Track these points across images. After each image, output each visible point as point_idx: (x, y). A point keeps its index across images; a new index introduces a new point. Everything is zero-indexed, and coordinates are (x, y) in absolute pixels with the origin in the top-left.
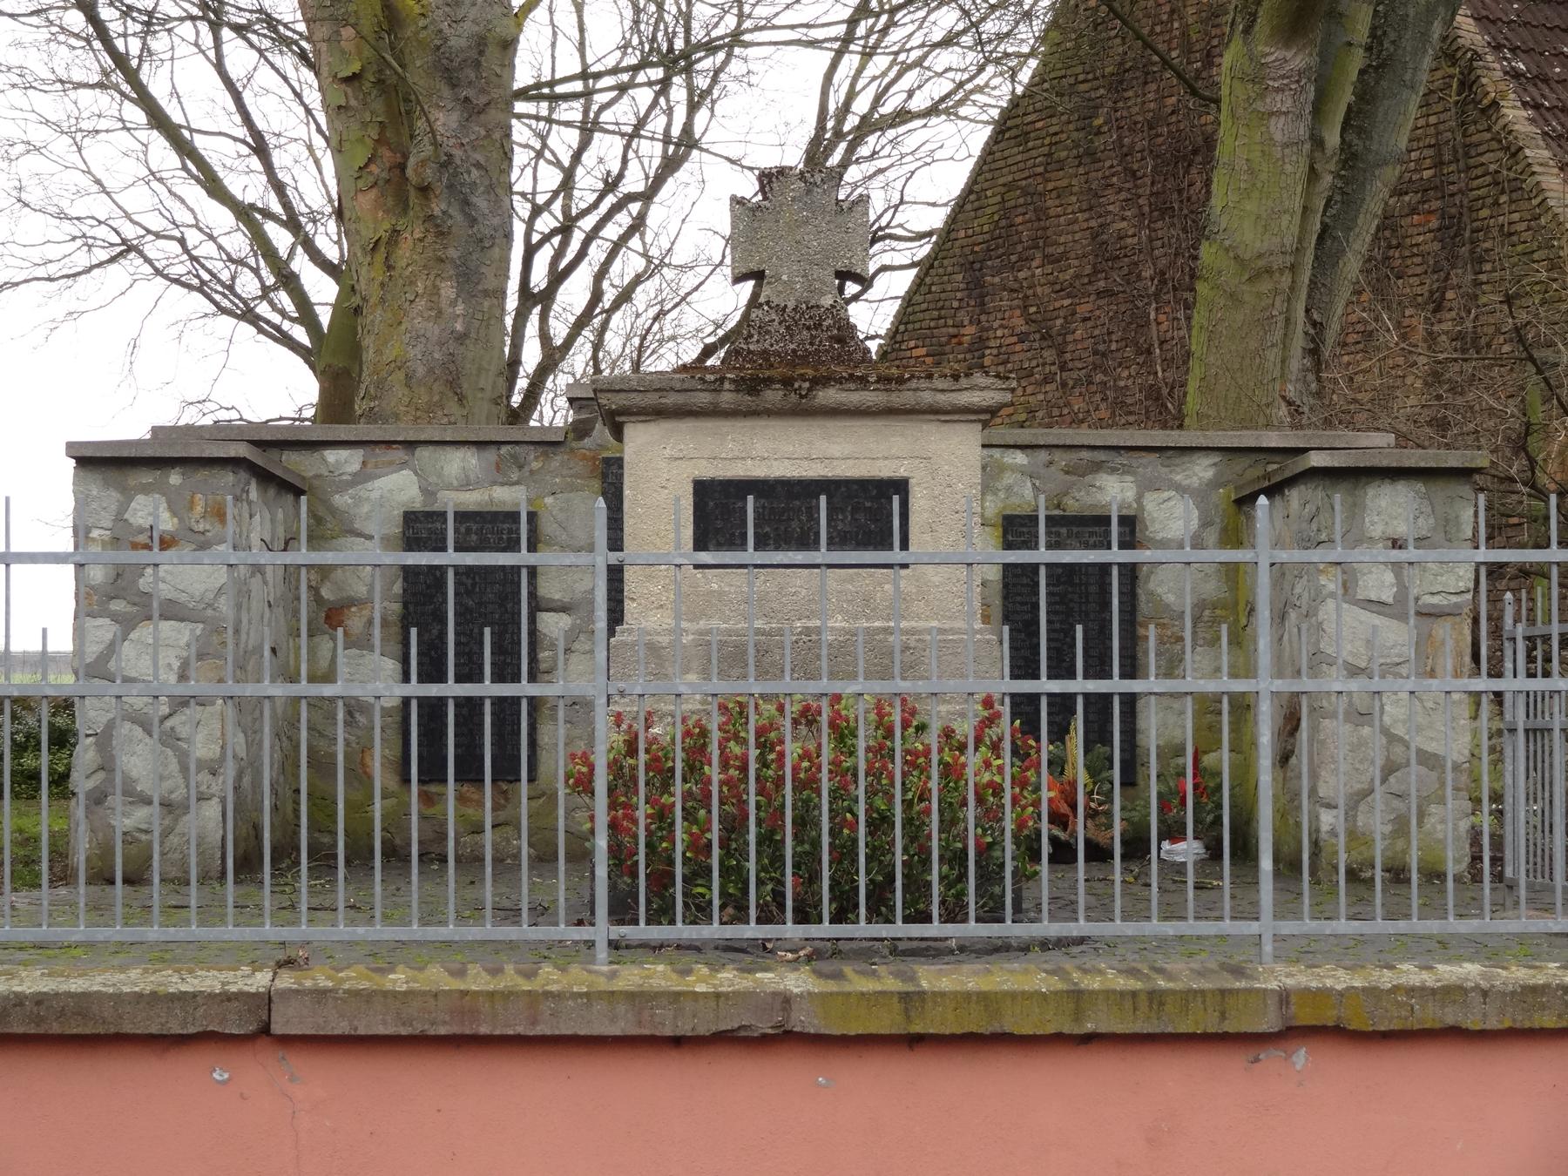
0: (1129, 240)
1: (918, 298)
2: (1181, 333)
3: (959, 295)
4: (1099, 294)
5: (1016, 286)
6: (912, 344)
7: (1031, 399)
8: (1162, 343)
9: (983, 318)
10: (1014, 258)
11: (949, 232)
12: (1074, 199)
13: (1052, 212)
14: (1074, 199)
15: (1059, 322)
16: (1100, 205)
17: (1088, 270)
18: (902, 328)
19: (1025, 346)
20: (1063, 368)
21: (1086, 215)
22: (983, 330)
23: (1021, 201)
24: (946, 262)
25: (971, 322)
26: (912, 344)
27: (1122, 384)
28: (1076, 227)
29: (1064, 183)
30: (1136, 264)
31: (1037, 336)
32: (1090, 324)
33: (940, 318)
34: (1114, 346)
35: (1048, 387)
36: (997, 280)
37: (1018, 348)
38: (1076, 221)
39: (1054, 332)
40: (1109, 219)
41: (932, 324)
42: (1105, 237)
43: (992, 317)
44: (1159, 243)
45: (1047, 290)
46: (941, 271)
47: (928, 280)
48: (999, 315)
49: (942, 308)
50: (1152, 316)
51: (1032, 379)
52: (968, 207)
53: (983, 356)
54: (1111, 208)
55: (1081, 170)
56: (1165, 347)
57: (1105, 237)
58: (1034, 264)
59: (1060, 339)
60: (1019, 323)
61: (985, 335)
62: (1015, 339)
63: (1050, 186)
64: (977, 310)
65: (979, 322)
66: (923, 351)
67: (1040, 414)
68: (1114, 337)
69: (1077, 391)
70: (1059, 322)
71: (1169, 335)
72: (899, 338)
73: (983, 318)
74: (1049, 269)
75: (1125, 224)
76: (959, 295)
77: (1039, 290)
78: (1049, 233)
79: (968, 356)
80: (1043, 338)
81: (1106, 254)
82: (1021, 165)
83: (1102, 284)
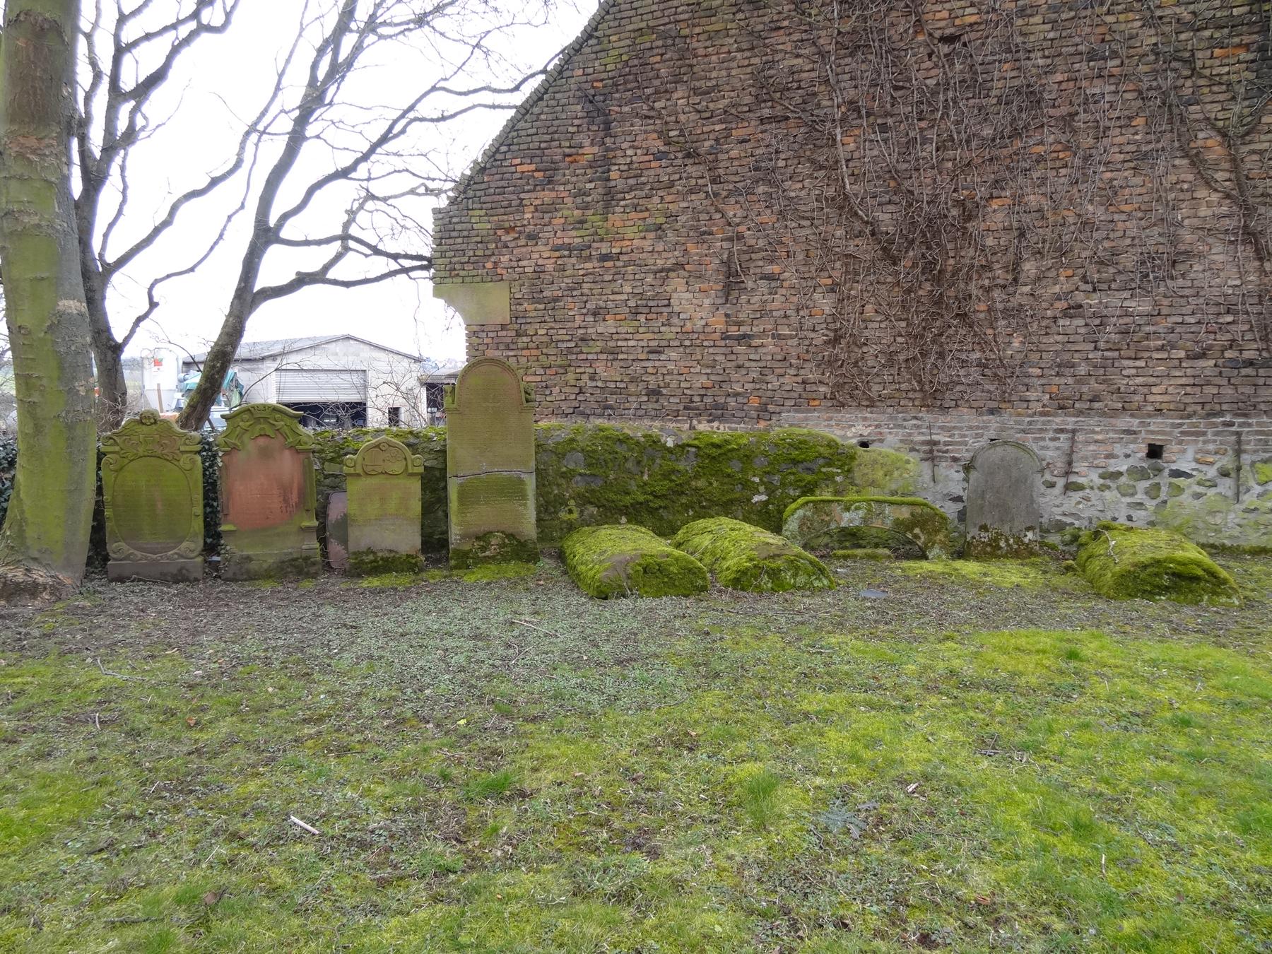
0: (806, 75)
1: (522, 125)
2: (876, 152)
3: (576, 122)
4: (762, 121)
5: (652, 113)
6: (518, 161)
7: (671, 206)
8: (848, 161)
9: (608, 140)
10: (648, 91)
11: (560, 72)
12: (732, 41)
13: (701, 52)
14: (732, 41)
15: (707, 144)
16: (766, 46)
17: (748, 99)
18: (504, 149)
19: (664, 162)
20: (714, 182)
21: (747, 54)
22: (607, 150)
23: (660, 43)
24: (557, 96)
25: (592, 144)
26: (518, 161)
27: (793, 194)
28: (734, 64)
29: (716, 27)
30: (815, 94)
31: (680, 155)
32: (748, 145)
33: (552, 140)
34: (781, 163)
35: (693, 197)
36: (626, 109)
37: (653, 164)
38: (733, 59)
39: (702, 151)
40: (778, 57)
41: (543, 145)
42: (772, 72)
43: (618, 140)
44: (847, 77)
45: (694, 116)
46: (553, 103)
47: (536, 110)
48: (628, 138)
49: (556, 132)
50: (839, 138)
51: (674, 190)
52: (586, 50)
53: (609, 170)
54: (780, 47)
55: (740, 16)
56: (851, 164)
57: (772, 72)
58: (675, 96)
59: (711, 158)
60: (657, 145)
61: (611, 154)
62: (651, 157)
63: (697, 30)
64: (602, 134)
65: (604, 143)
66: (533, 167)
67: (683, 218)
68: (783, 156)
69: (732, 200)
70: (707, 144)
71: (856, 155)
72: (498, 156)
73: (608, 140)
74: (697, 100)
75: (800, 60)
76: (576, 122)
77: (682, 118)
78: (695, 69)
79: (588, 171)
80: (688, 156)
81: (765, 90)
82: (659, 14)
83: (766, 112)
